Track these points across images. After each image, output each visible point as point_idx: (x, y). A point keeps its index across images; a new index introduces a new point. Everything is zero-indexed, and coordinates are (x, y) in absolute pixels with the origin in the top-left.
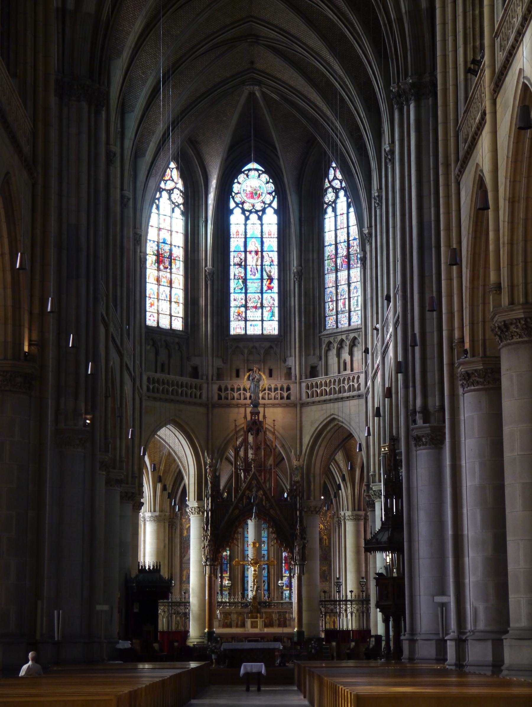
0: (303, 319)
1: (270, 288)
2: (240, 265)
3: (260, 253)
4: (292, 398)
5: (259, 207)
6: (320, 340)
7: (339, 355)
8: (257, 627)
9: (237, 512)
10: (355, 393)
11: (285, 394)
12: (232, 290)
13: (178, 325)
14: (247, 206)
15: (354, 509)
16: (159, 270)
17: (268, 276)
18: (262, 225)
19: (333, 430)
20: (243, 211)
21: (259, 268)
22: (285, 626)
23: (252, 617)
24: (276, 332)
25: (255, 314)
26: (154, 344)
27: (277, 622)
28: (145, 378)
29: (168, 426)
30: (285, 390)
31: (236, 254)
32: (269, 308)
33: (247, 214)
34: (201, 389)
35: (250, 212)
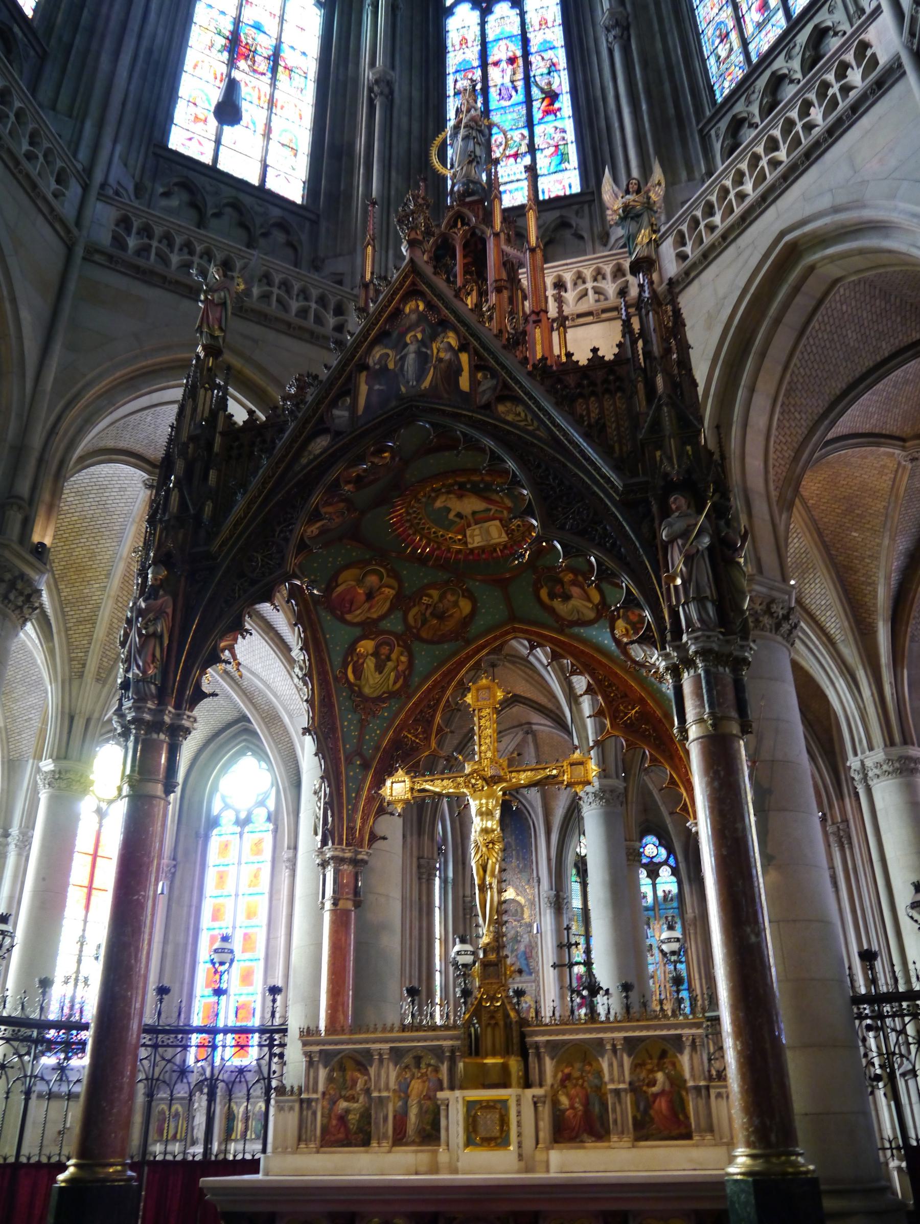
0: (644, 107)
1: (547, 112)
3: (520, 61)
8: (499, 1140)
9: (321, 444)
15: (890, 742)
17: (542, 90)
18: (522, 14)
19: (793, 318)
21: (520, 85)
22: (677, 1128)
24: (576, 189)
27: (628, 1100)
30: (609, 277)
31: (458, 76)
32: (552, 149)
34: (339, 311)
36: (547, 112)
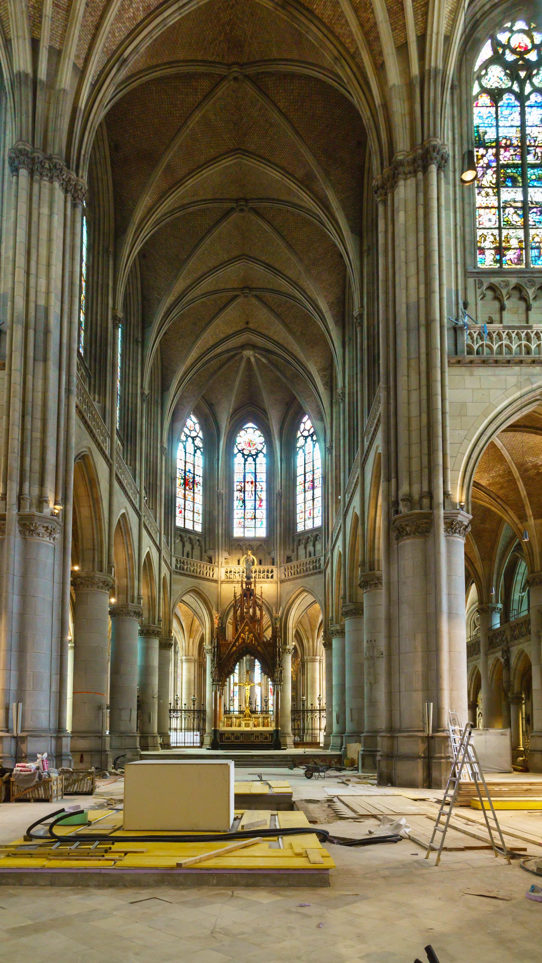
2: (241, 491)
4: (275, 577)
5: (253, 452)
6: (293, 538)
7: (305, 548)
8: (249, 726)
9: (235, 648)
10: (318, 570)
11: (270, 575)
12: (235, 507)
13: (199, 528)
14: (246, 452)
16: (185, 490)
18: (255, 464)
20: (244, 455)
21: (253, 493)
22: (268, 726)
23: (246, 720)
25: (250, 522)
26: (182, 540)
28: (174, 559)
29: (191, 594)
31: (238, 484)
33: (246, 457)
35: (248, 456)
36: (260, 506)
